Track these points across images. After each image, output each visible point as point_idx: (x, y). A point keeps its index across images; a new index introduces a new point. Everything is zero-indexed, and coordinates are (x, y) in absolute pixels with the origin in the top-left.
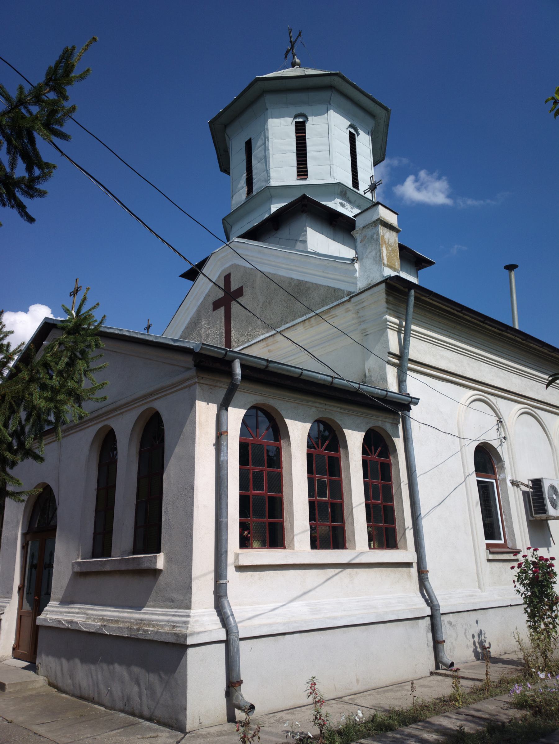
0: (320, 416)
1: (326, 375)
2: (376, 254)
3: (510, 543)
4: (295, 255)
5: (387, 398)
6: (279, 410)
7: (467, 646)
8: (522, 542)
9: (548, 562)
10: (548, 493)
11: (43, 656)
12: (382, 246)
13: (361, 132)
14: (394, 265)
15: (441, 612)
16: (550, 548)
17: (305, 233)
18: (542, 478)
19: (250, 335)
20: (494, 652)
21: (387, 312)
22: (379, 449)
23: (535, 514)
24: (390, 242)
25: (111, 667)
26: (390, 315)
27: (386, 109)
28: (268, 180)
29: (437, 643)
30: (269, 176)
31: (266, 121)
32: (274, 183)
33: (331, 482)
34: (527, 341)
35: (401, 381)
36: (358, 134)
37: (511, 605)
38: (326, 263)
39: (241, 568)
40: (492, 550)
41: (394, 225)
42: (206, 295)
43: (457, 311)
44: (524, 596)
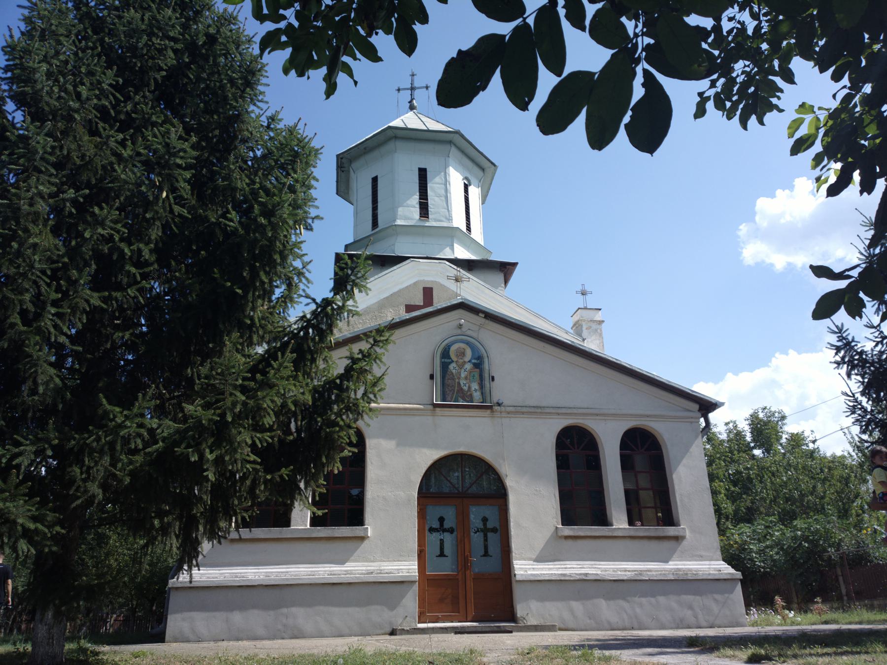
11: (534, 605)
25: (653, 600)
28: (450, 219)
31: (446, 167)
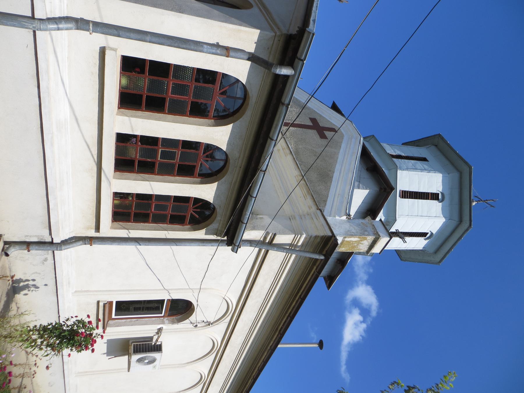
0: (231, 161)
1: (268, 165)
2: (353, 232)
3: (112, 323)
4: (352, 175)
5: (240, 223)
6: (241, 119)
7: (25, 274)
8: (113, 333)
9: (90, 347)
10: (150, 356)
12: (359, 237)
13: (427, 241)
14: (343, 247)
15: (55, 252)
16: (106, 355)
17: (365, 188)
18: (162, 353)
19: (291, 139)
20: (20, 297)
21: (308, 235)
22: (197, 216)
23: (134, 345)
24: (360, 245)
26: (306, 238)
27: (440, 262)
29: (28, 245)
30: (403, 170)
31: (440, 172)
32: (399, 172)
33: (173, 165)
34: (269, 350)
35: (251, 243)
36: (425, 239)
37: (59, 317)
38: (346, 196)
39: (103, 52)
40: (107, 306)
41: (372, 251)
42: (321, 115)
43: (301, 295)
44: (63, 323)
